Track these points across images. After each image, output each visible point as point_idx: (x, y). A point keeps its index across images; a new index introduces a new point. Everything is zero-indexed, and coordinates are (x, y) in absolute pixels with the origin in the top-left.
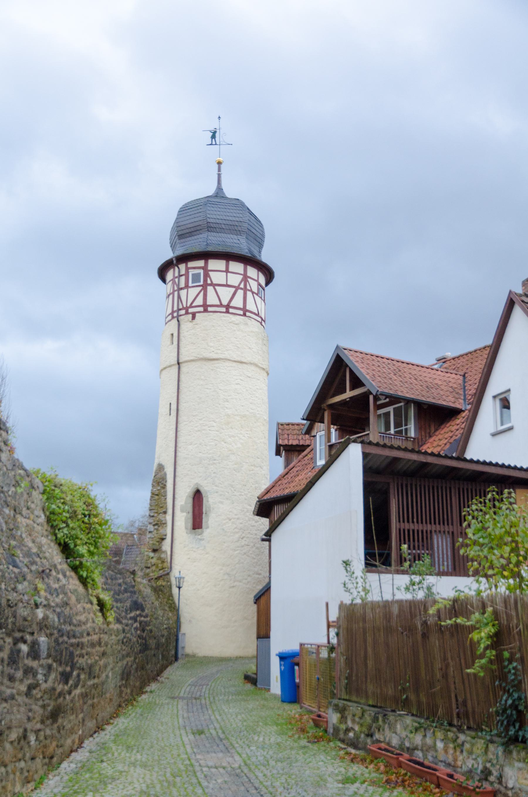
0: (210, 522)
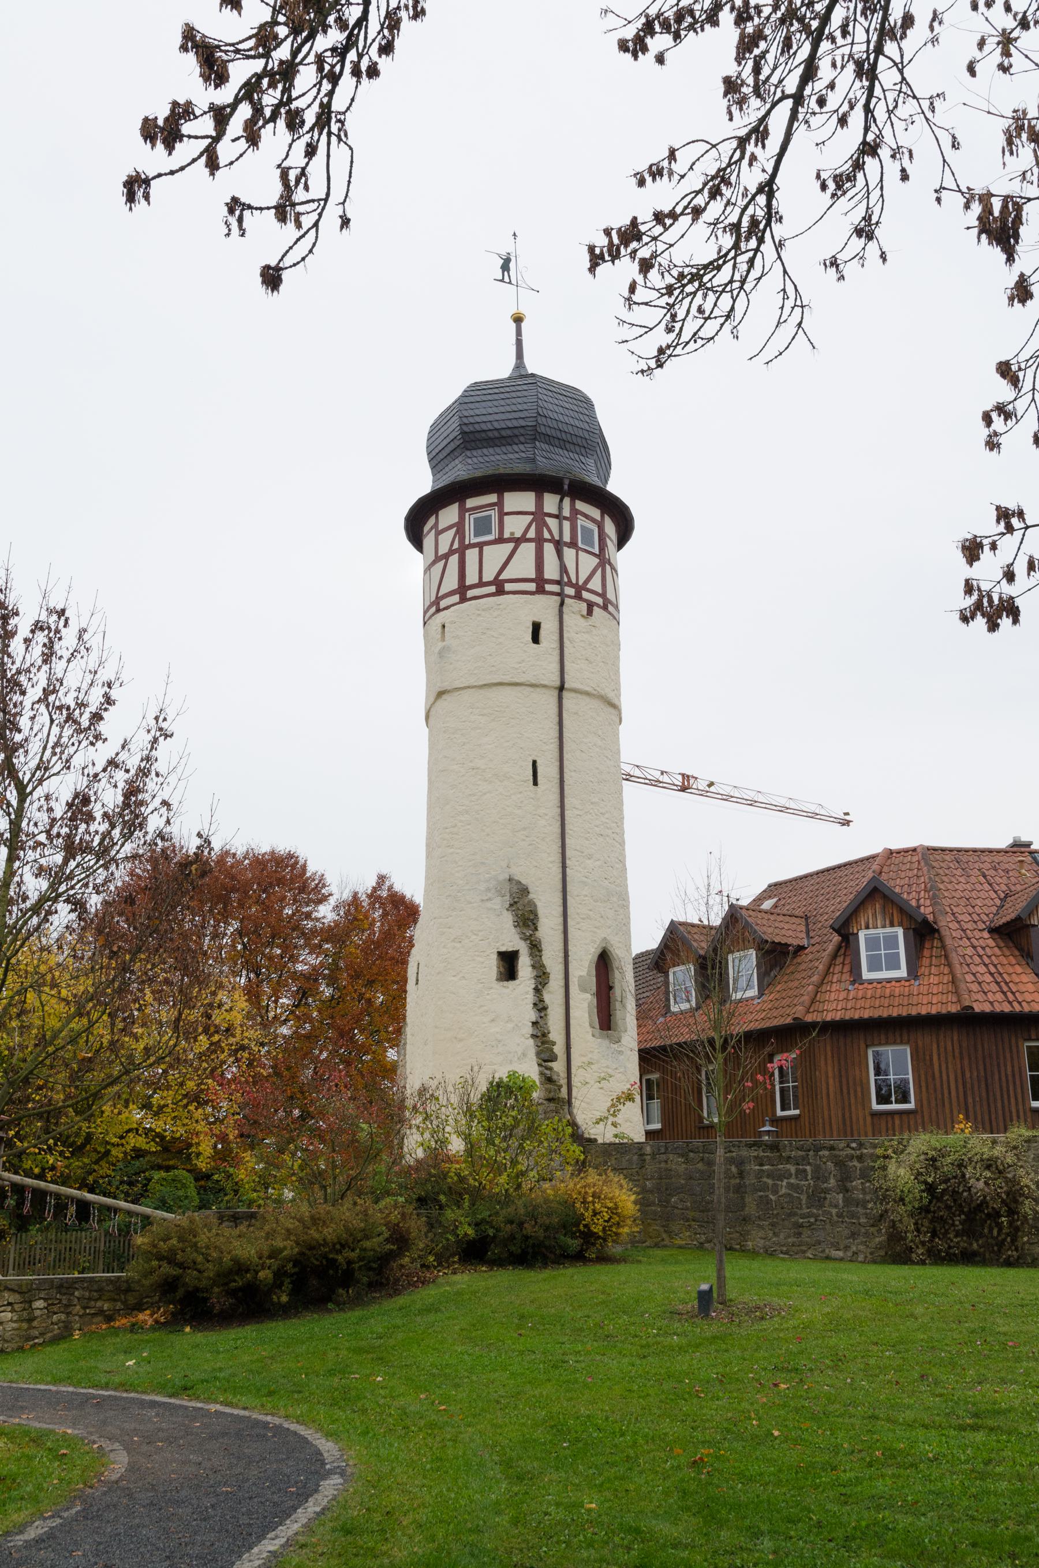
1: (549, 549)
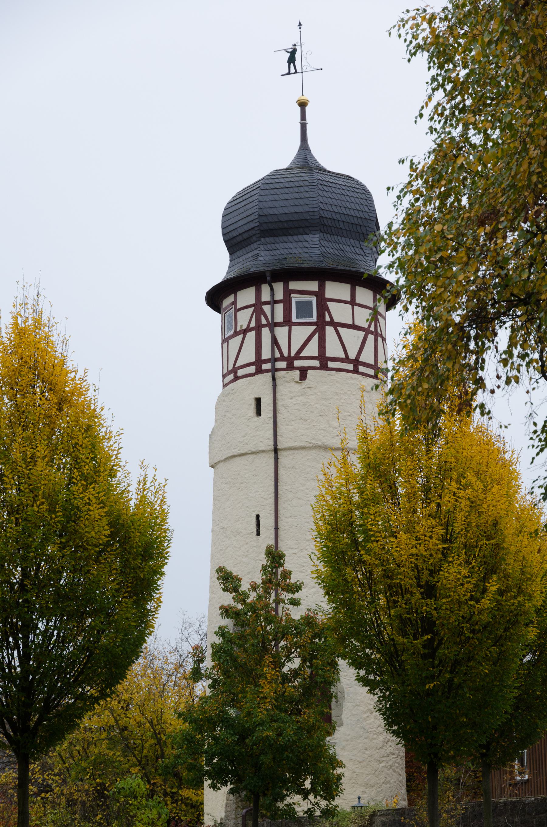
0: (344, 716)
1: (266, 332)
